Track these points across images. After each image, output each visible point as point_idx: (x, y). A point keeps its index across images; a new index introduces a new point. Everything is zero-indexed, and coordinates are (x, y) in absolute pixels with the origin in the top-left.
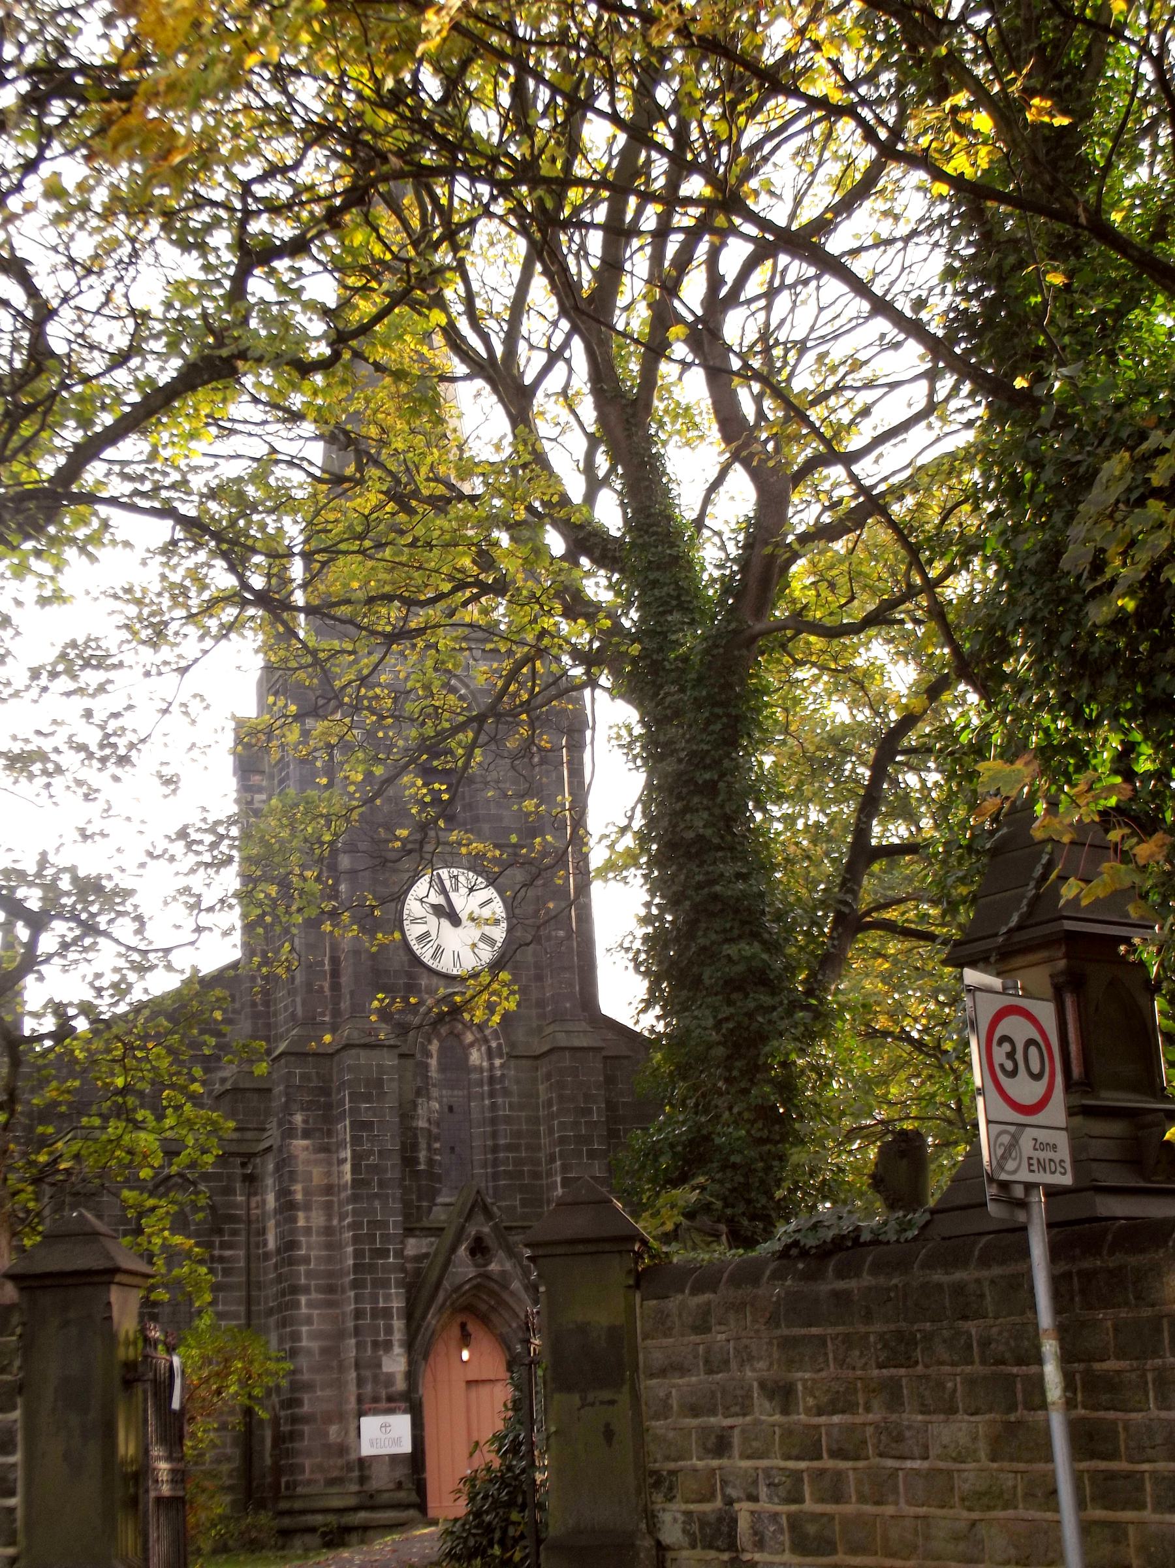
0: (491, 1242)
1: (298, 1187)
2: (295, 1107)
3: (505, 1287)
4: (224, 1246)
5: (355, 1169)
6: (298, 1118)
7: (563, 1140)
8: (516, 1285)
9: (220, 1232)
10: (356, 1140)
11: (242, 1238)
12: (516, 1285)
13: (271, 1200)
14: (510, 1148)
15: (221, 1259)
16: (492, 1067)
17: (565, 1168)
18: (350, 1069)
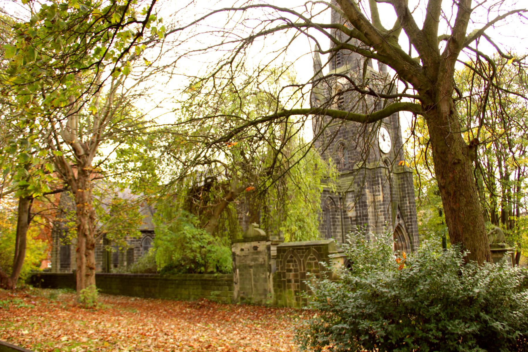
0: (400, 216)
1: (367, 201)
2: (366, 181)
3: (402, 226)
4: (338, 215)
5: (383, 197)
6: (366, 184)
7: (408, 193)
8: (403, 226)
9: (336, 211)
10: (383, 190)
11: (340, 213)
12: (403, 226)
13: (350, 203)
14: (395, 194)
15: (337, 218)
16: (390, 176)
17: (409, 200)
18: (381, 173)
